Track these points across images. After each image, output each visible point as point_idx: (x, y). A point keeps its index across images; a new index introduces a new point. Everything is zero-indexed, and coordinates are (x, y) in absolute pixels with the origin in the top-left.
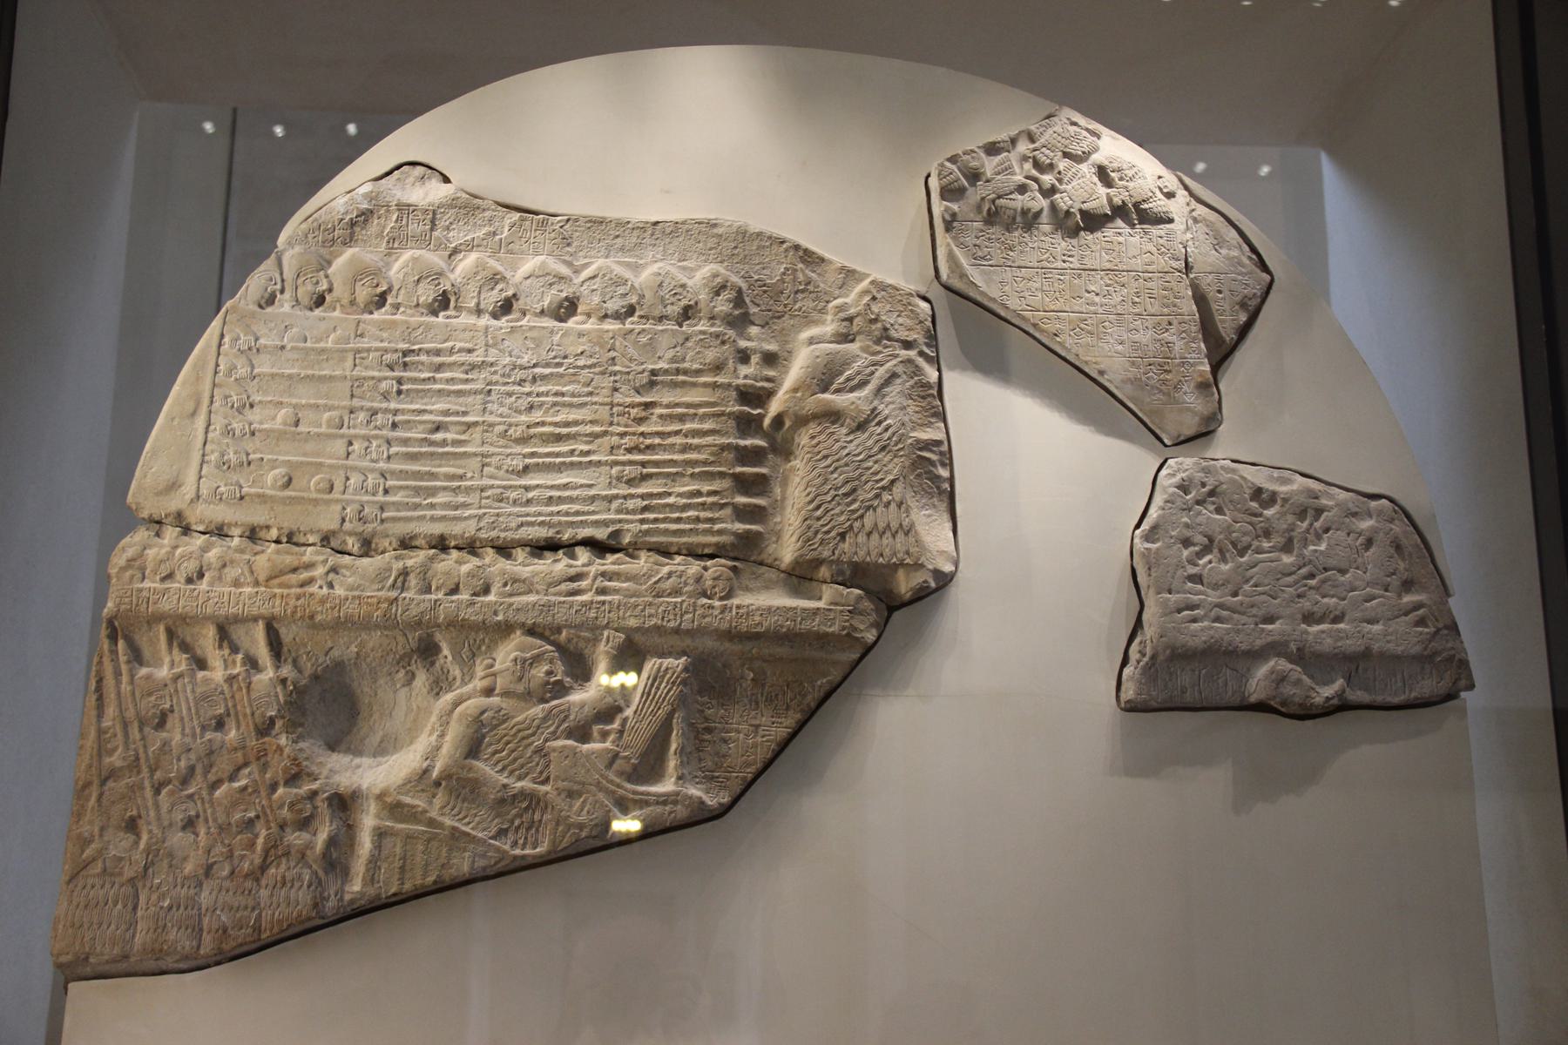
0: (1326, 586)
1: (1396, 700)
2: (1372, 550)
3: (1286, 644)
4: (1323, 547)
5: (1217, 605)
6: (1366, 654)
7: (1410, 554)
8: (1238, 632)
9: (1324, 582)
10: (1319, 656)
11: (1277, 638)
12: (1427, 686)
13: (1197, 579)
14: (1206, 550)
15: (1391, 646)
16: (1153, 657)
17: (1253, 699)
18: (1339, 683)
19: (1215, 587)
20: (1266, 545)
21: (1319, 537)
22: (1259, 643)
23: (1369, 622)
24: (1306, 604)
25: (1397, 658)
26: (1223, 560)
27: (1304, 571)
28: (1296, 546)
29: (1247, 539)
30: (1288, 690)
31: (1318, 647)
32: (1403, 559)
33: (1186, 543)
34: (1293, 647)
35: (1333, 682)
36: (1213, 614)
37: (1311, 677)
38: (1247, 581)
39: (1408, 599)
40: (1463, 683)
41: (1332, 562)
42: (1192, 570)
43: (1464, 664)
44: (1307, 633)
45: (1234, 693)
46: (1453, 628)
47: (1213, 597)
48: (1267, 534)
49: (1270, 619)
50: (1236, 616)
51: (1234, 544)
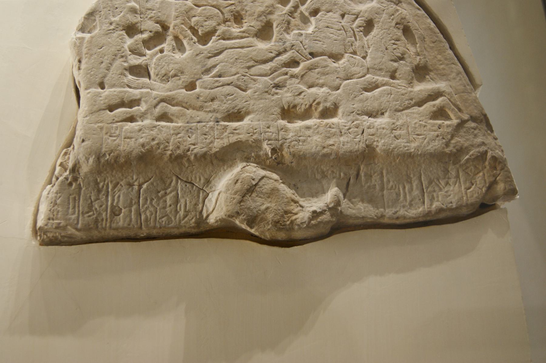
0: (313, 76)
1: (415, 212)
2: (375, 31)
3: (258, 144)
4: (311, 29)
5: (163, 100)
6: (368, 154)
7: (423, 39)
8: (189, 131)
9: (310, 69)
10: (300, 157)
11: (243, 137)
12: (454, 193)
13: (140, 71)
14: (157, 38)
15: (401, 142)
16: (75, 169)
17: (212, 220)
18: (332, 193)
19: (165, 78)
20: (235, 30)
21: (305, 20)
22: (218, 145)
23: (370, 115)
24: (285, 96)
25: (410, 156)
26: (179, 46)
27: (284, 57)
28: (275, 30)
29: (211, 24)
30: (257, 203)
31: (302, 148)
32: (414, 44)
33: (131, 30)
34: (267, 148)
35: (324, 192)
36: (158, 111)
37: (295, 187)
38: (207, 71)
39: (422, 88)
40: (501, 187)
41: (318, 47)
42: (135, 60)
43: (498, 163)
44: (286, 130)
45: (187, 213)
46: (483, 120)
47: (160, 89)
48: (238, 18)
49: (236, 115)
50: (189, 112)
51: (194, 31)
